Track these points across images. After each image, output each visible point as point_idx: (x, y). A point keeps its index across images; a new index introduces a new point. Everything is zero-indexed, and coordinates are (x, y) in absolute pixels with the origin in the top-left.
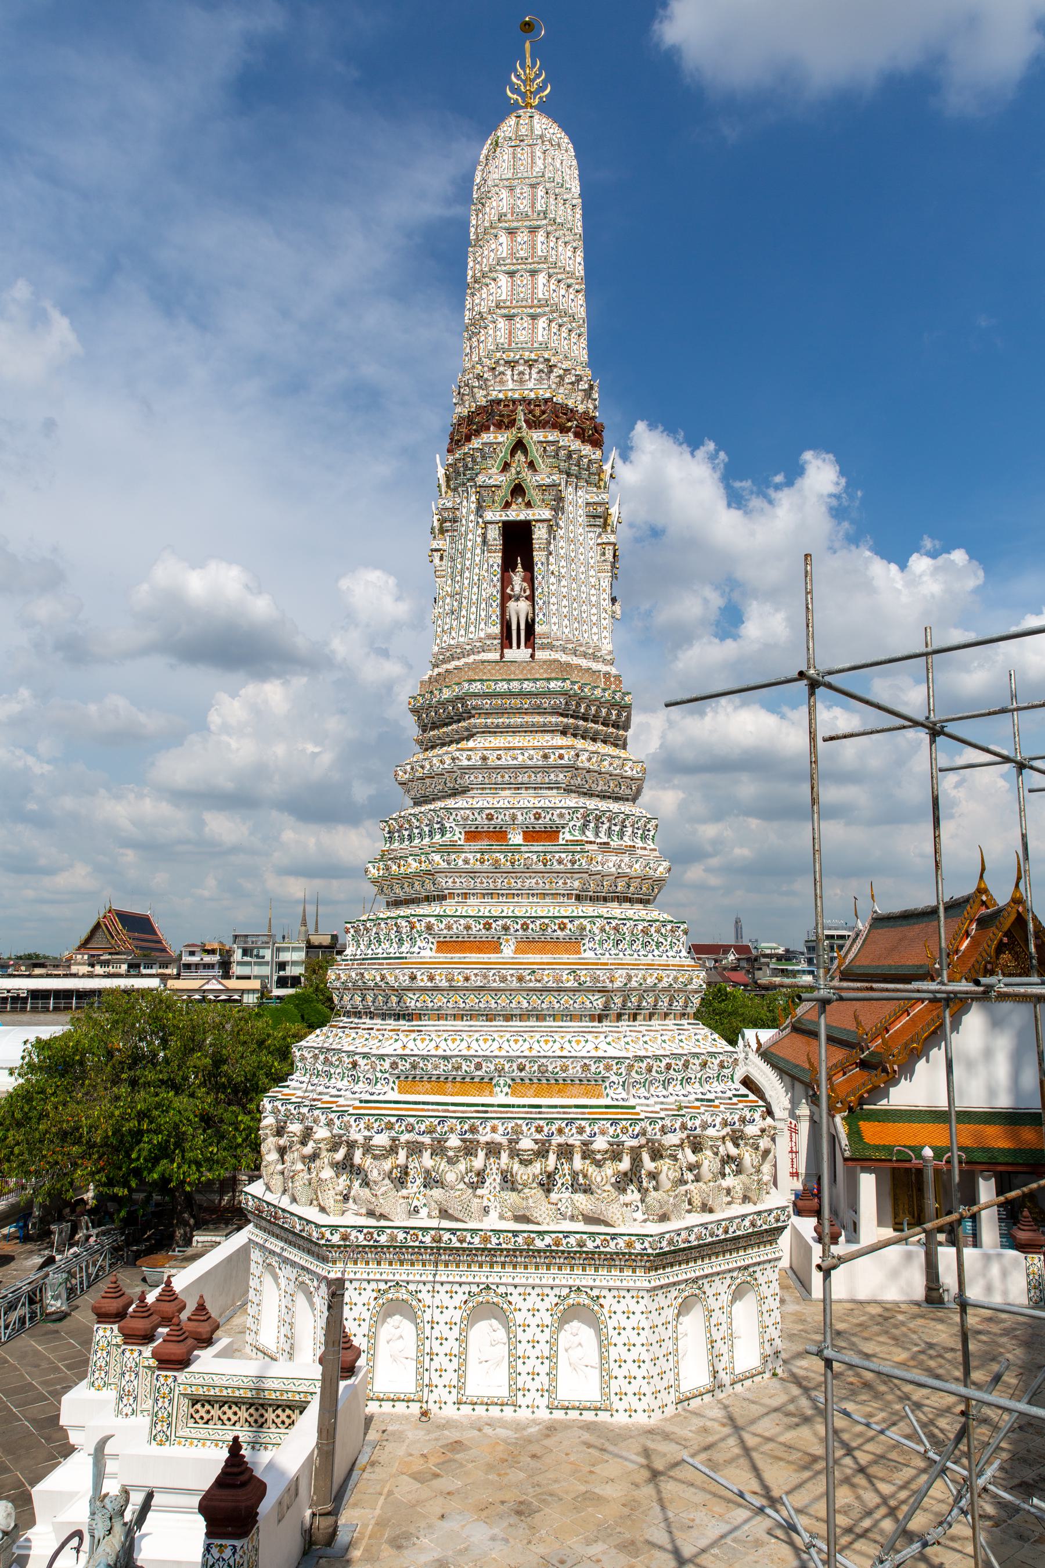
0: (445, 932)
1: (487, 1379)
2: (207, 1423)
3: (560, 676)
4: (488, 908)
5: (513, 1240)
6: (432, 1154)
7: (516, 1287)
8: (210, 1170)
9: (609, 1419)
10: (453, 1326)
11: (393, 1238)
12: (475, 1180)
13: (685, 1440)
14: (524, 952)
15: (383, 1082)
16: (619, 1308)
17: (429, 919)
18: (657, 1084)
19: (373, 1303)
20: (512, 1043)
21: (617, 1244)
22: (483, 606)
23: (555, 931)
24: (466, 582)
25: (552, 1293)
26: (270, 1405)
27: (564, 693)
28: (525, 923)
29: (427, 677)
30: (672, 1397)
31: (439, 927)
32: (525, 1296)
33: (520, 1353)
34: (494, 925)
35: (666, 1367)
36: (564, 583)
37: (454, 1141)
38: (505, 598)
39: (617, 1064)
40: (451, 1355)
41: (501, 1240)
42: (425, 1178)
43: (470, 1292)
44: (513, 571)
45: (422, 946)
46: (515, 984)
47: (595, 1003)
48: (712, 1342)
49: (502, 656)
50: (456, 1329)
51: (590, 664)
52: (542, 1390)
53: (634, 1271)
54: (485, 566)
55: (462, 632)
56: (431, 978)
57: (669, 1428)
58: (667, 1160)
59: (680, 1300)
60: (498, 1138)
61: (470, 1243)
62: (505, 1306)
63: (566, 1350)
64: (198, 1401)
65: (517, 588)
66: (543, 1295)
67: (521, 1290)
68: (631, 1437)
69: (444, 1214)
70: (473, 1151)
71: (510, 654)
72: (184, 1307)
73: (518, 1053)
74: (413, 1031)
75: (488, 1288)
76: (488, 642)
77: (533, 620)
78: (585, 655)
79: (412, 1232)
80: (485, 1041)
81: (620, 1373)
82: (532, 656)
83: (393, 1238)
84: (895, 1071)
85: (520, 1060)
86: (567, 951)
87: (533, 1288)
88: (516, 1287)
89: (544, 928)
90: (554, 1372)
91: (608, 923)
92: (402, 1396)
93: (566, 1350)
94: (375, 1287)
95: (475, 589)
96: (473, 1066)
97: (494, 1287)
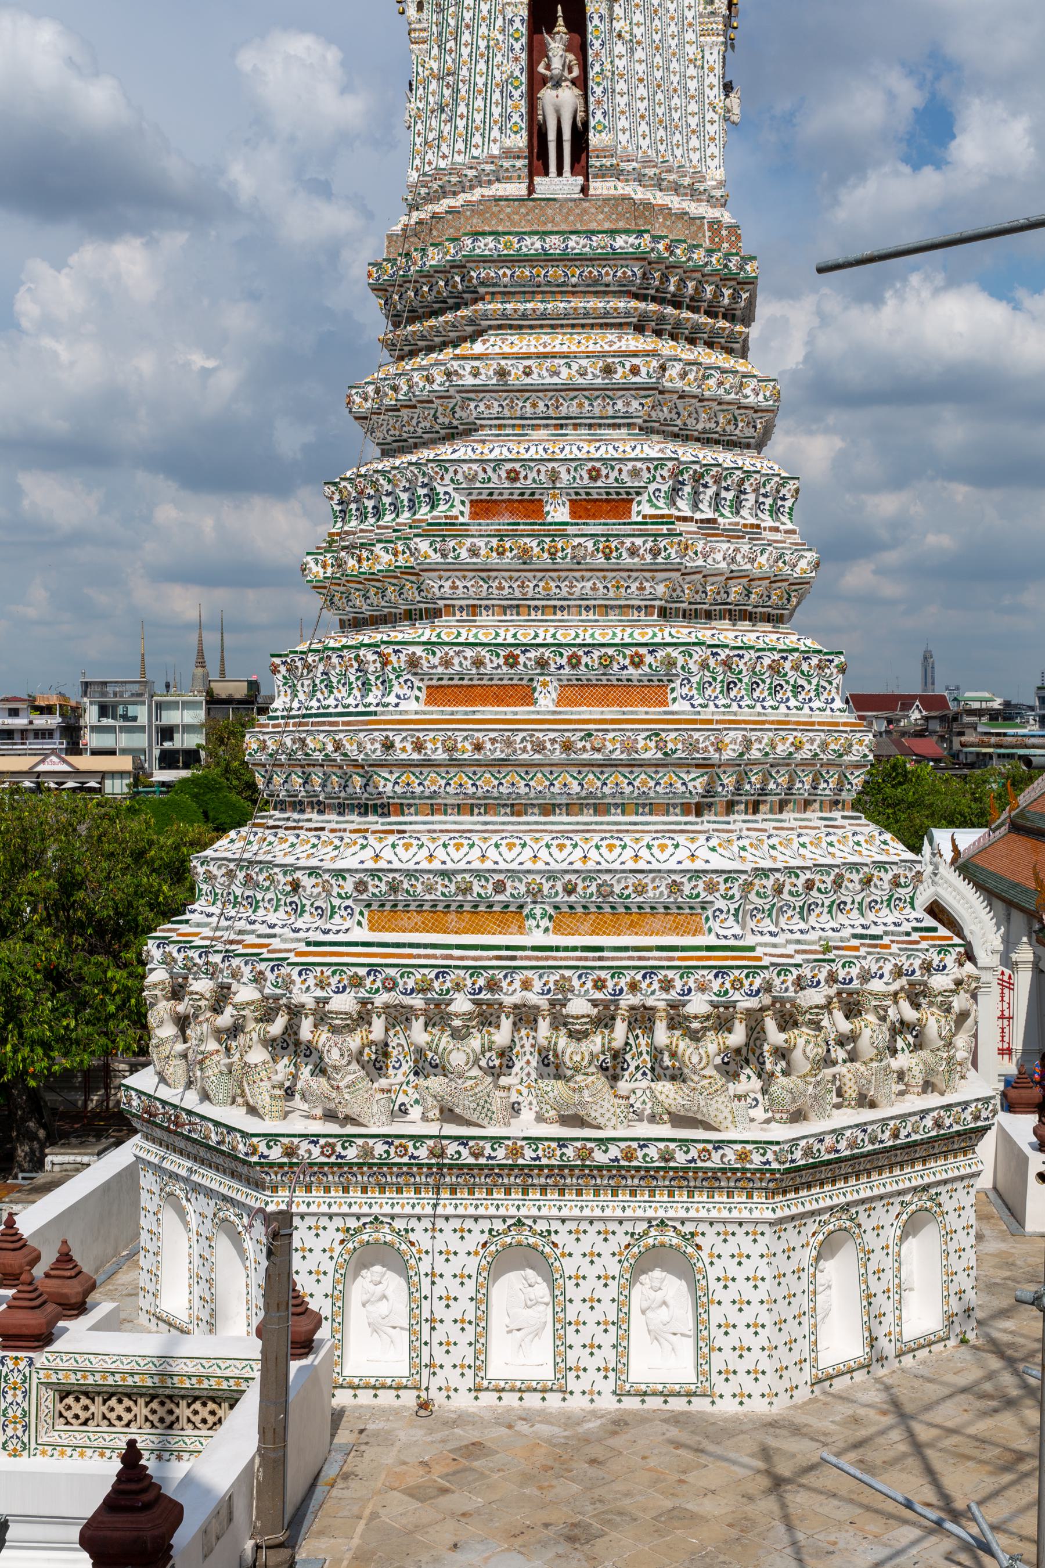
0: (440, 670)
1: (520, 1354)
2: (85, 1423)
3: (633, 227)
4: (512, 631)
5: (558, 1153)
6: (426, 1025)
7: (563, 1221)
8: (65, 1055)
10: (466, 1280)
12: (497, 1062)
13: (825, 1434)
14: (572, 703)
16: (726, 1250)
17: (412, 649)
18: (790, 913)
19: (338, 1249)
20: (554, 850)
21: (723, 1156)
22: (497, 96)
23: (625, 667)
24: (465, 51)
25: (620, 1230)
26: (183, 1397)
27: (640, 257)
28: (574, 656)
29: (397, 228)
30: (807, 1375)
31: (430, 661)
32: (577, 1235)
33: (571, 1316)
34: (522, 659)
35: (797, 1332)
36: (640, 54)
37: (461, 1004)
38: (535, 82)
39: (726, 881)
41: (540, 1153)
42: (416, 1061)
43: (491, 1230)
44: (550, 32)
45: (401, 693)
46: (558, 755)
47: (690, 785)
48: (869, 1296)
49: (531, 189)
50: (470, 1284)
51: (684, 205)
52: (606, 1369)
53: (750, 1196)
54: (499, 22)
55: (460, 145)
56: (419, 747)
57: (800, 1419)
58: (804, 1029)
59: (821, 1237)
60: (532, 998)
61: (489, 1158)
62: (547, 1250)
64: (68, 1394)
65: (557, 64)
66: (606, 1232)
67: (571, 1225)
68: (742, 1432)
69: (448, 1114)
70: (493, 1019)
71: (545, 186)
72: (37, 1258)
73: (564, 866)
74: (392, 832)
75: (519, 1223)
76: (506, 164)
77: (586, 124)
78: (676, 189)
79: (397, 1142)
80: (511, 847)
81: (726, 1343)
82: (584, 189)
83: (368, 1152)
85: (567, 877)
86: (645, 702)
88: (563, 1221)
89: (606, 663)
91: (714, 654)
92: (389, 1382)
93: (643, 1312)
94: (341, 1225)
95: (482, 66)
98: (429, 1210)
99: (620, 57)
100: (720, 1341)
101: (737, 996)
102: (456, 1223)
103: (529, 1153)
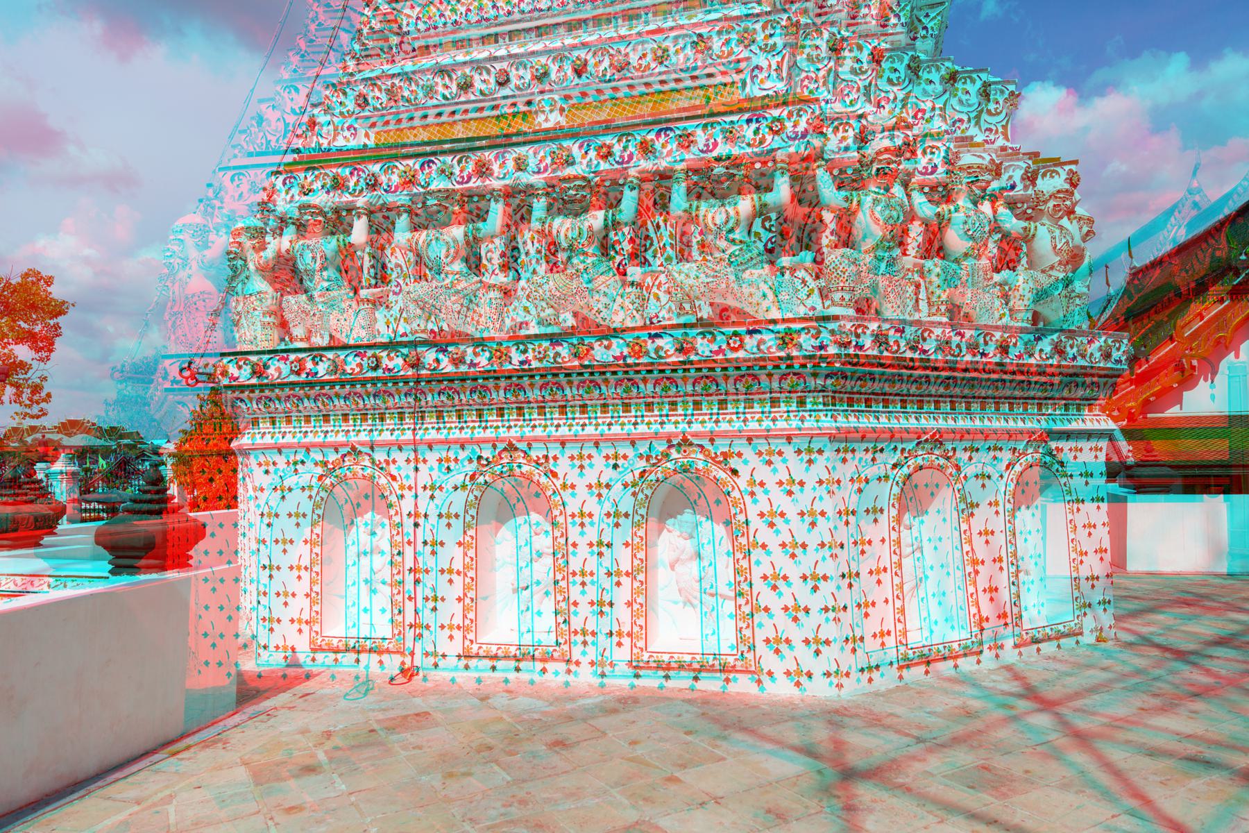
9: (753, 689)
11: (336, 367)
13: (919, 727)
15: (347, 133)
18: (853, 96)
21: (761, 342)
32: (581, 462)
40: (450, 571)
41: (530, 355)
48: (975, 562)
50: (458, 524)
52: (620, 634)
60: (526, 178)
63: (672, 567)
67: (572, 450)
79: (370, 353)
84: (1193, 368)
85: (575, 53)
87: (597, 445)
90: (641, 599)
93: (672, 567)
94: (319, 458)
96: (492, 80)
97: (522, 446)
98: (408, 435)
100: (766, 597)
101: (777, 142)
102: (440, 452)
103: (516, 357)
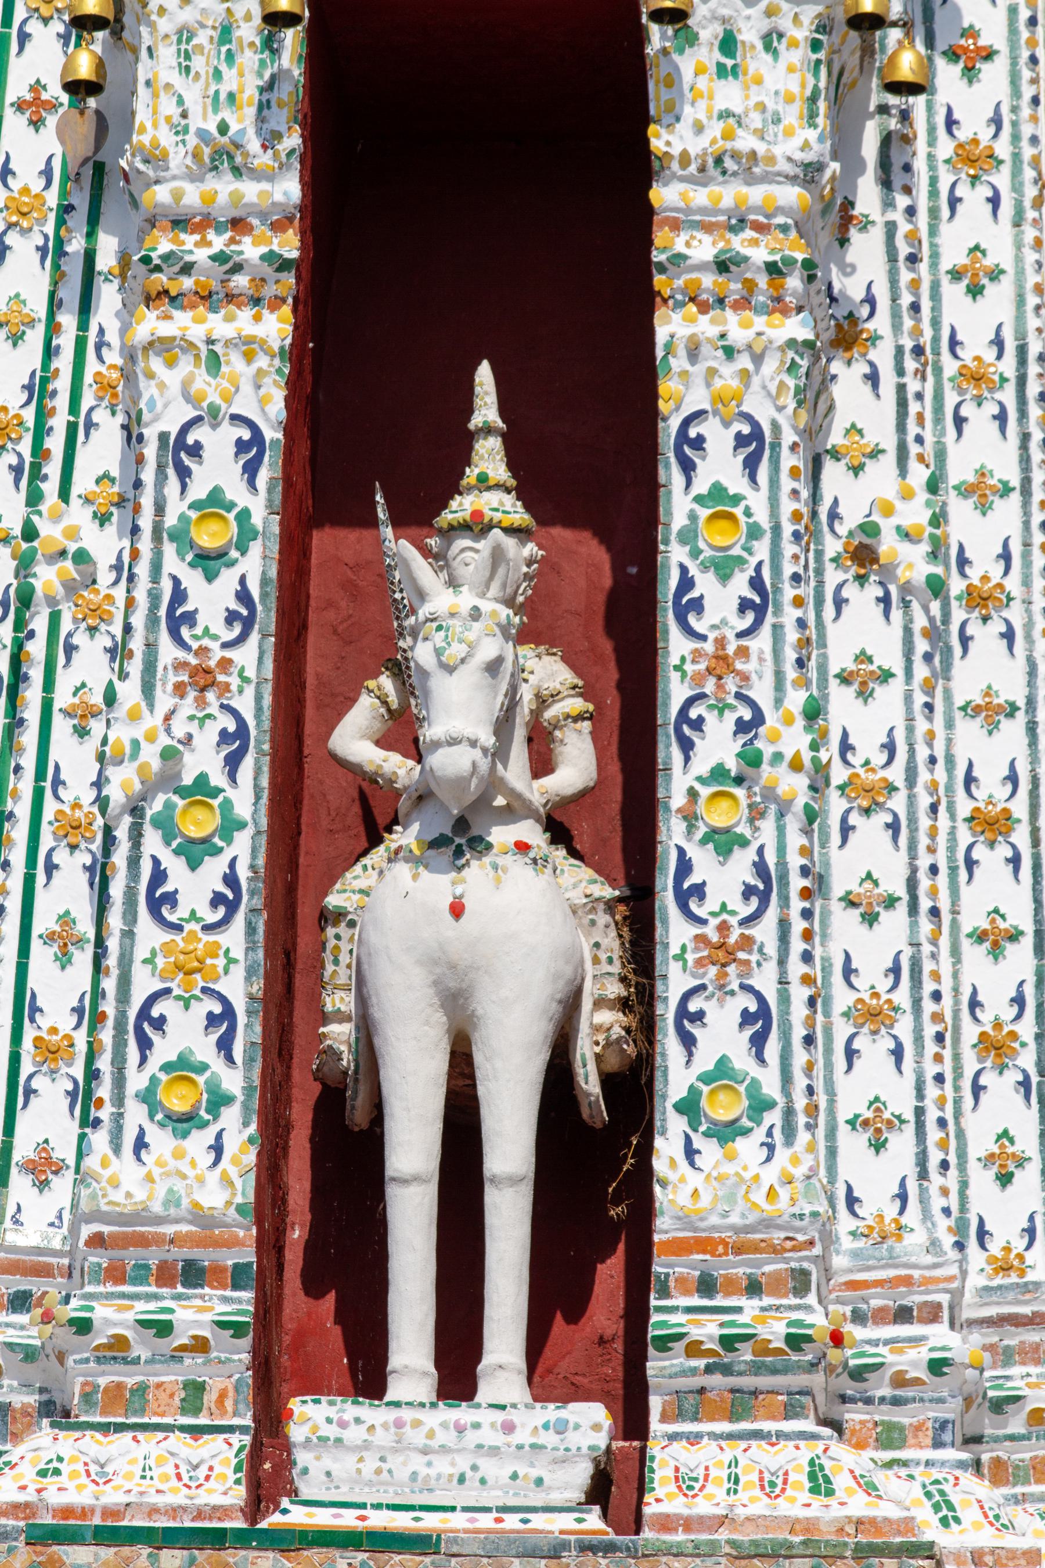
38: (320, 823)
44: (418, 512)
49: (268, 1473)
54: (102, 453)
65: (459, 714)
71: (358, 1455)
76: (113, 1315)
77: (633, 1087)
82: (616, 1487)
99: (865, 679)
